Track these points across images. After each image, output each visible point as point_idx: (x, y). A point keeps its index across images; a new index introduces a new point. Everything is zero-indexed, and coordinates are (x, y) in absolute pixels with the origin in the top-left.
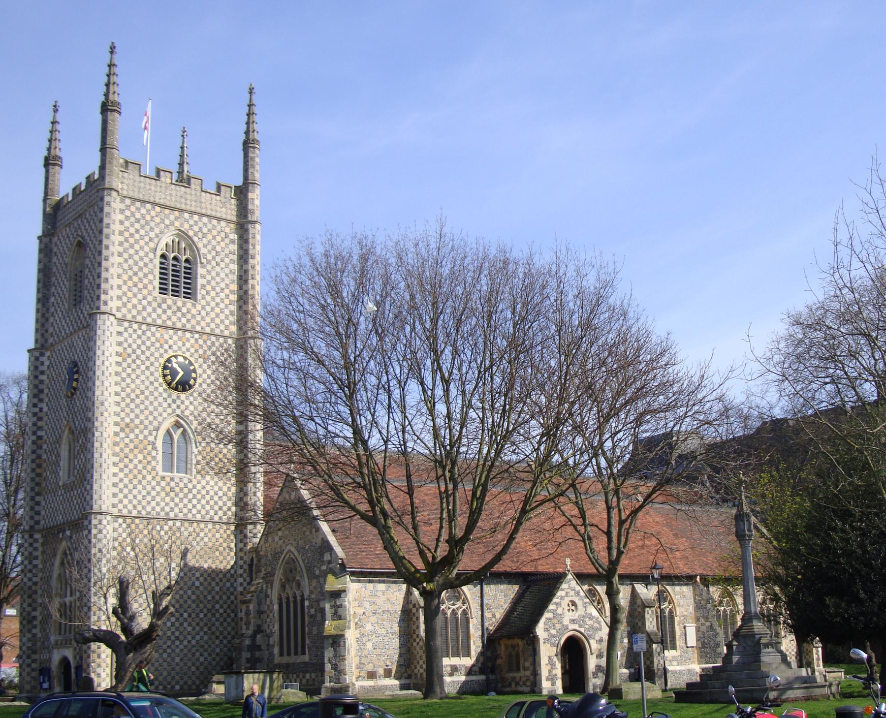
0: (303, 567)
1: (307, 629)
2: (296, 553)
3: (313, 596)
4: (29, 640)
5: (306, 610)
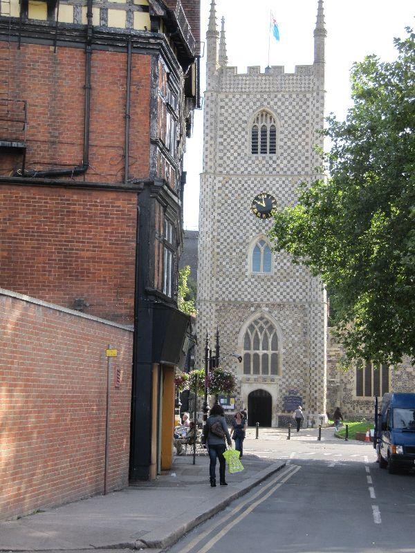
1: (390, 383)
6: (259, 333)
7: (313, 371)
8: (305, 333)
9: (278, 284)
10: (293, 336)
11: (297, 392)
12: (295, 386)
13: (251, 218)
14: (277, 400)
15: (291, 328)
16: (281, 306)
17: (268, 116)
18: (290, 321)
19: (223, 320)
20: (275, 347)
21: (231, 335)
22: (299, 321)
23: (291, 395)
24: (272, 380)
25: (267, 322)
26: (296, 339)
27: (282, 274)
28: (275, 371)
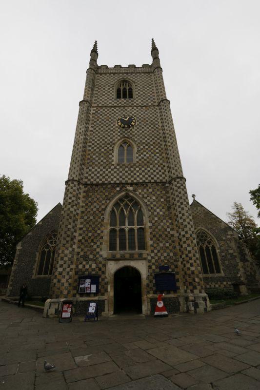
0: (213, 236)
2: (206, 230)
3: (222, 248)
4: (70, 253)
5: (218, 254)
6: (125, 210)
7: (185, 242)
8: (169, 208)
9: (140, 169)
10: (158, 210)
11: (167, 268)
12: (166, 261)
13: (117, 129)
14: (148, 278)
15: (155, 203)
16: (144, 184)
17: (127, 84)
18: (154, 198)
19: (90, 199)
20: (140, 222)
21: (97, 212)
22: (162, 197)
23: (163, 271)
24: (141, 255)
25: (132, 199)
26: (161, 213)
27: (143, 162)
28: (143, 246)
